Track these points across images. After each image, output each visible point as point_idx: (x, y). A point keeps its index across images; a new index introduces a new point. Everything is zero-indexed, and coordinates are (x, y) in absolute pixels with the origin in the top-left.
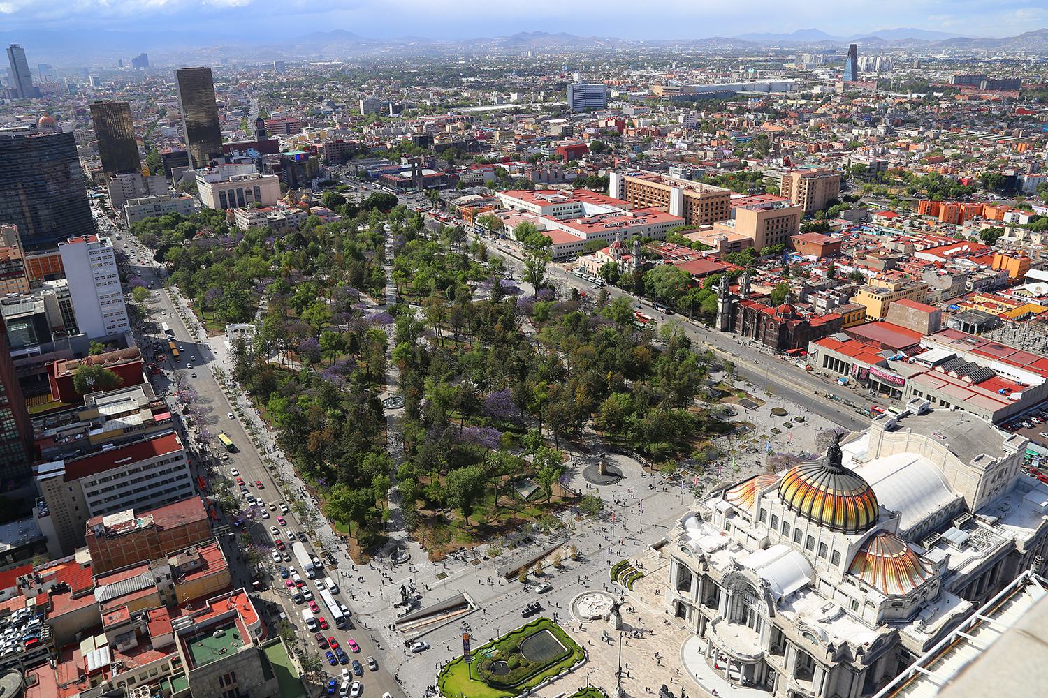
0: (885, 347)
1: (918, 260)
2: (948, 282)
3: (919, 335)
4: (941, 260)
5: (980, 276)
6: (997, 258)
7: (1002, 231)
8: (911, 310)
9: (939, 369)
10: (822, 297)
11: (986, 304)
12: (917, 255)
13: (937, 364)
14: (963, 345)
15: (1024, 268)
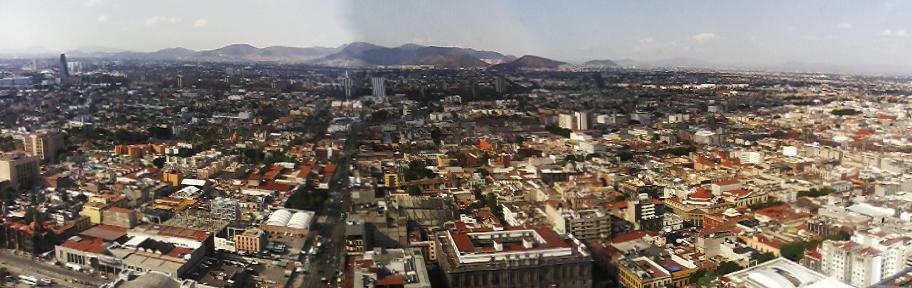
0: (105, 241)
1: (119, 183)
2: (139, 194)
3: (125, 229)
4: (133, 180)
5: (158, 187)
6: (165, 175)
7: (165, 159)
8: (117, 214)
9: (141, 249)
10: (60, 214)
11: (162, 204)
12: (118, 179)
13: (139, 246)
14: (152, 232)
15: (180, 180)
